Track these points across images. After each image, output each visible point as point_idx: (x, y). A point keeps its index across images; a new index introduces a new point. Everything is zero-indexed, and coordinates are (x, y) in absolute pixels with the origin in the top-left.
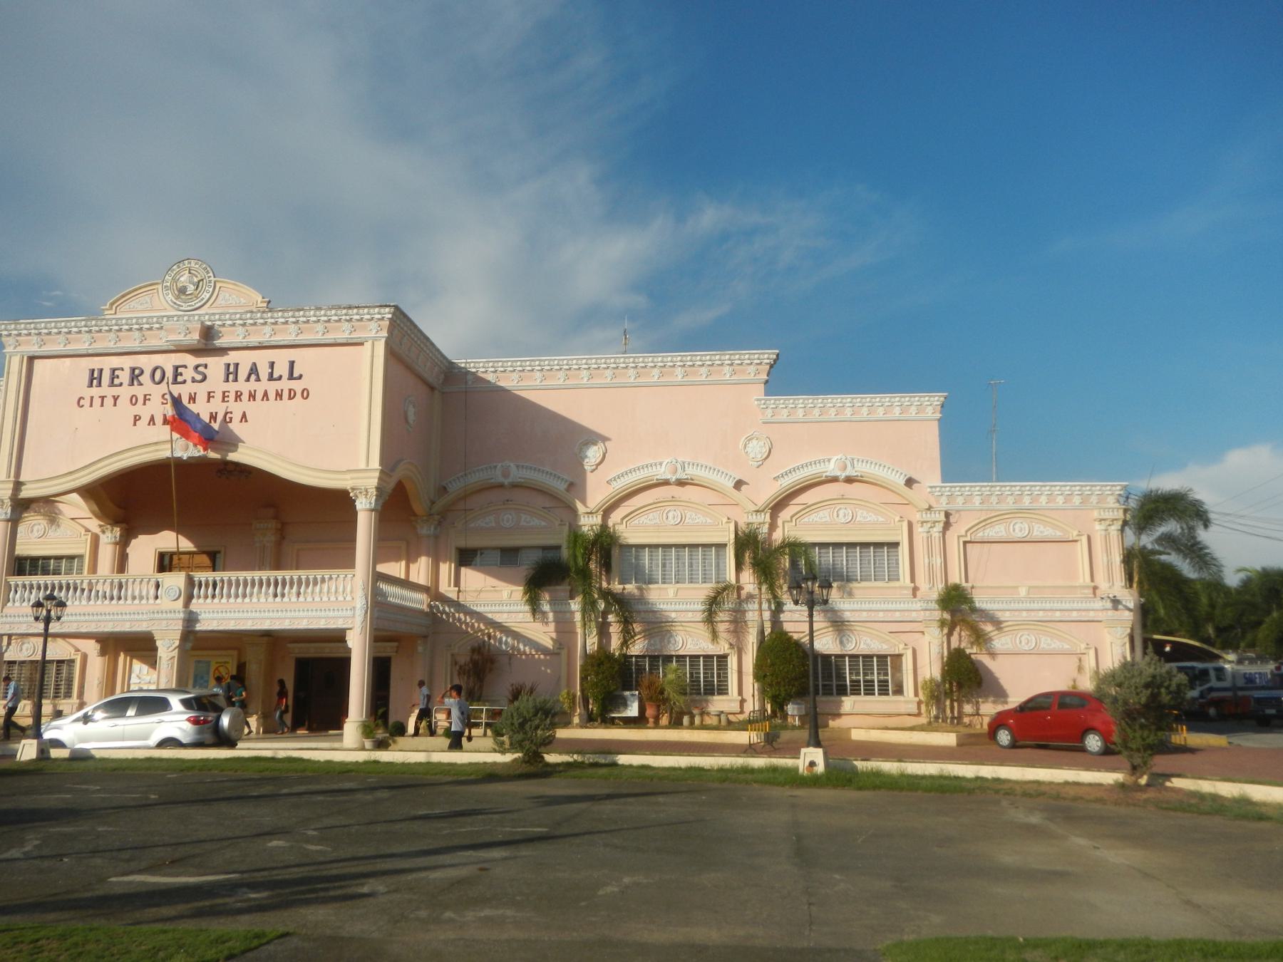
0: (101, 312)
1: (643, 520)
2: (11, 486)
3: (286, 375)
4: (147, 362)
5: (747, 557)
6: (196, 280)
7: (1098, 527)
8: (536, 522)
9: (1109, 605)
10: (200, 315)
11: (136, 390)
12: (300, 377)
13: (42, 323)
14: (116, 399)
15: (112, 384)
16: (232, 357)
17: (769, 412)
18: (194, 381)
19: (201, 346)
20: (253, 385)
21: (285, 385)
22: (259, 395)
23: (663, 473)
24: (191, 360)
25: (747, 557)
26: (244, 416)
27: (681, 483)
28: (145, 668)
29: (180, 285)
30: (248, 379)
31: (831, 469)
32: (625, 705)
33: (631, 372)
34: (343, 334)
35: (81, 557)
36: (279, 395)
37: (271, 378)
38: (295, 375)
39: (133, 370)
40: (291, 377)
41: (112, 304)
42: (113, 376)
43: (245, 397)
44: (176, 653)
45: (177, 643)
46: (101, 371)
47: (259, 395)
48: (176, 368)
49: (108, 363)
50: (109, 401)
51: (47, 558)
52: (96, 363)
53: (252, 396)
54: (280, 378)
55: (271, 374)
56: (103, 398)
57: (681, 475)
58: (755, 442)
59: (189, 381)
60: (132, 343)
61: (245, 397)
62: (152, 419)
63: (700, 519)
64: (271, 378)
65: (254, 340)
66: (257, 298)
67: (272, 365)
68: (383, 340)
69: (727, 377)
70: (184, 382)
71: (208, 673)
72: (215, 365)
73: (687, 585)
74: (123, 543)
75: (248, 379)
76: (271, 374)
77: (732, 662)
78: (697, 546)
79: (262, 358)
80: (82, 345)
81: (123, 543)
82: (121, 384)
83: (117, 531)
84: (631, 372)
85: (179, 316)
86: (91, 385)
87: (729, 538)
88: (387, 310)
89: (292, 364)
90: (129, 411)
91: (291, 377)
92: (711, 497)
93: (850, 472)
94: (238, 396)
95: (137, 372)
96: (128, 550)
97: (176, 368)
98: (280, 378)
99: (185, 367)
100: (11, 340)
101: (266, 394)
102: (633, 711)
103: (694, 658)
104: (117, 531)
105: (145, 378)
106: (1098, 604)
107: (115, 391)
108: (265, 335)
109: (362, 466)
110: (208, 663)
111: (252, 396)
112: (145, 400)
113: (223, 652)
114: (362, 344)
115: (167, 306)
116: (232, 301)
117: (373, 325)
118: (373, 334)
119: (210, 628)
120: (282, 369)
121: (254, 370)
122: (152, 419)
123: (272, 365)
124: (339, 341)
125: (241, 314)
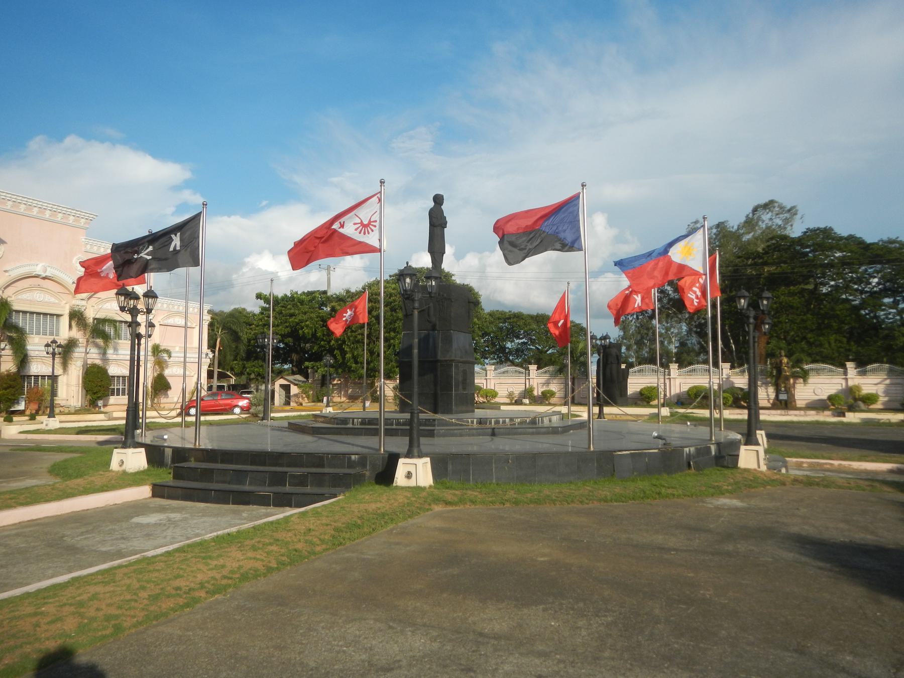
1: (26, 296)
5: (74, 324)
17: (88, 247)
23: (38, 270)
25: (74, 324)
27: (44, 278)
32: (18, 403)
33: (22, 206)
57: (48, 274)
63: (53, 300)
73: (41, 336)
77: (62, 381)
78: (45, 314)
84: (22, 206)
92: (58, 288)
102: (21, 406)
103: (43, 377)
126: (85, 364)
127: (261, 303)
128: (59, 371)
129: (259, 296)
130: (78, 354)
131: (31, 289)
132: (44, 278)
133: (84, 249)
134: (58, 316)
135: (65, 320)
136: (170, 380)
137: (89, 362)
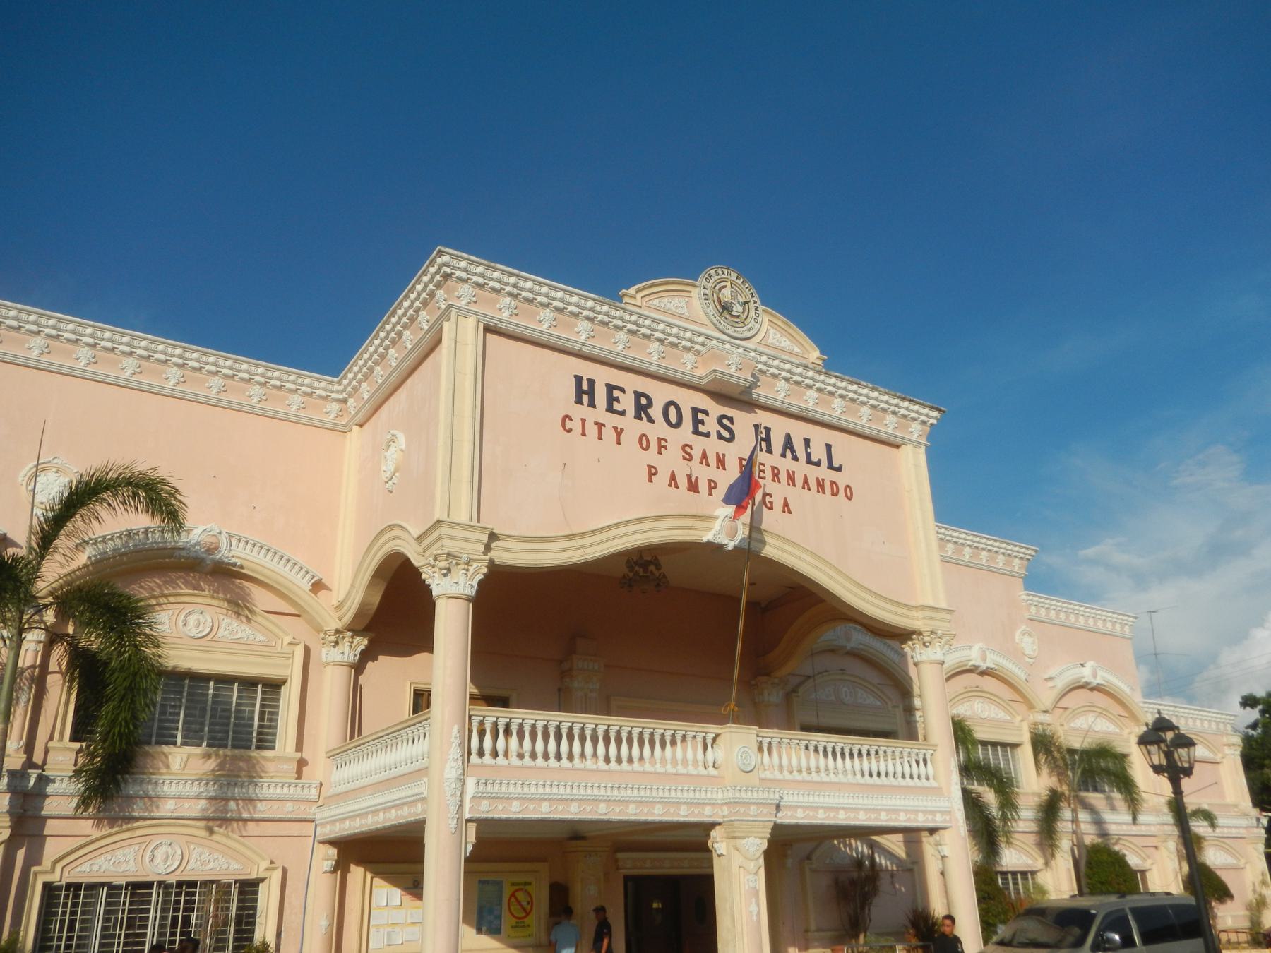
0: (620, 299)
2: (485, 538)
4: (660, 394)
6: (742, 300)
7: (1227, 751)
8: (871, 700)
9: (1255, 822)
10: (746, 349)
11: (643, 426)
12: (839, 469)
13: (530, 283)
14: (619, 432)
15: (610, 409)
16: (764, 418)
17: (1033, 610)
18: (720, 437)
19: (735, 394)
20: (786, 464)
21: (823, 472)
24: (716, 409)
25: (1042, 758)
26: (786, 504)
28: (397, 893)
29: (724, 300)
30: (783, 455)
31: (1086, 674)
34: (889, 425)
35: (274, 686)
36: (820, 485)
37: (809, 462)
38: (836, 464)
39: (638, 395)
40: (831, 467)
41: (638, 291)
42: (611, 399)
43: (783, 476)
44: (762, 861)
45: (765, 846)
46: (592, 383)
48: (695, 411)
49: (603, 376)
50: (608, 433)
51: (205, 678)
52: (588, 370)
53: (791, 478)
54: (818, 464)
55: (808, 455)
56: (600, 425)
57: (989, 664)
58: (1026, 638)
59: (714, 435)
60: (651, 355)
61: (783, 476)
62: (673, 478)
63: (1002, 715)
64: (809, 462)
65: (795, 404)
66: (814, 355)
67: (807, 442)
68: (923, 448)
69: (1000, 565)
70: (707, 435)
71: (500, 904)
72: (744, 422)
74: (358, 668)
75: (783, 455)
76: (808, 455)
79: (799, 431)
80: (580, 334)
81: (358, 668)
82: (623, 413)
83: (362, 643)
85: (720, 341)
86: (579, 401)
87: (1026, 739)
88: (935, 414)
89: (829, 447)
90: (633, 459)
91: (831, 467)
93: (1099, 681)
94: (776, 476)
95: (644, 401)
96: (361, 679)
97: (695, 411)
98: (818, 464)
99: (706, 413)
100: (466, 289)
101: (806, 481)
104: (362, 643)
105: (656, 412)
106: (1244, 822)
108: (809, 401)
109: (931, 603)
110: (499, 884)
112: (660, 447)
113: (527, 866)
114: (898, 447)
115: (705, 321)
116: (776, 348)
117: (916, 427)
118: (915, 437)
119: (793, 821)
120: (818, 453)
121: (788, 444)
122: (673, 478)
123: (807, 442)
124: (882, 436)
125: (794, 364)
126: (1080, 844)
127: (1254, 714)
128: (1040, 863)
129: (1249, 702)
130: (1064, 824)
131: (968, 694)
132: (983, 673)
133: (1027, 615)
134: (1014, 746)
135: (1026, 753)
136: (1226, 877)
137: (1088, 840)
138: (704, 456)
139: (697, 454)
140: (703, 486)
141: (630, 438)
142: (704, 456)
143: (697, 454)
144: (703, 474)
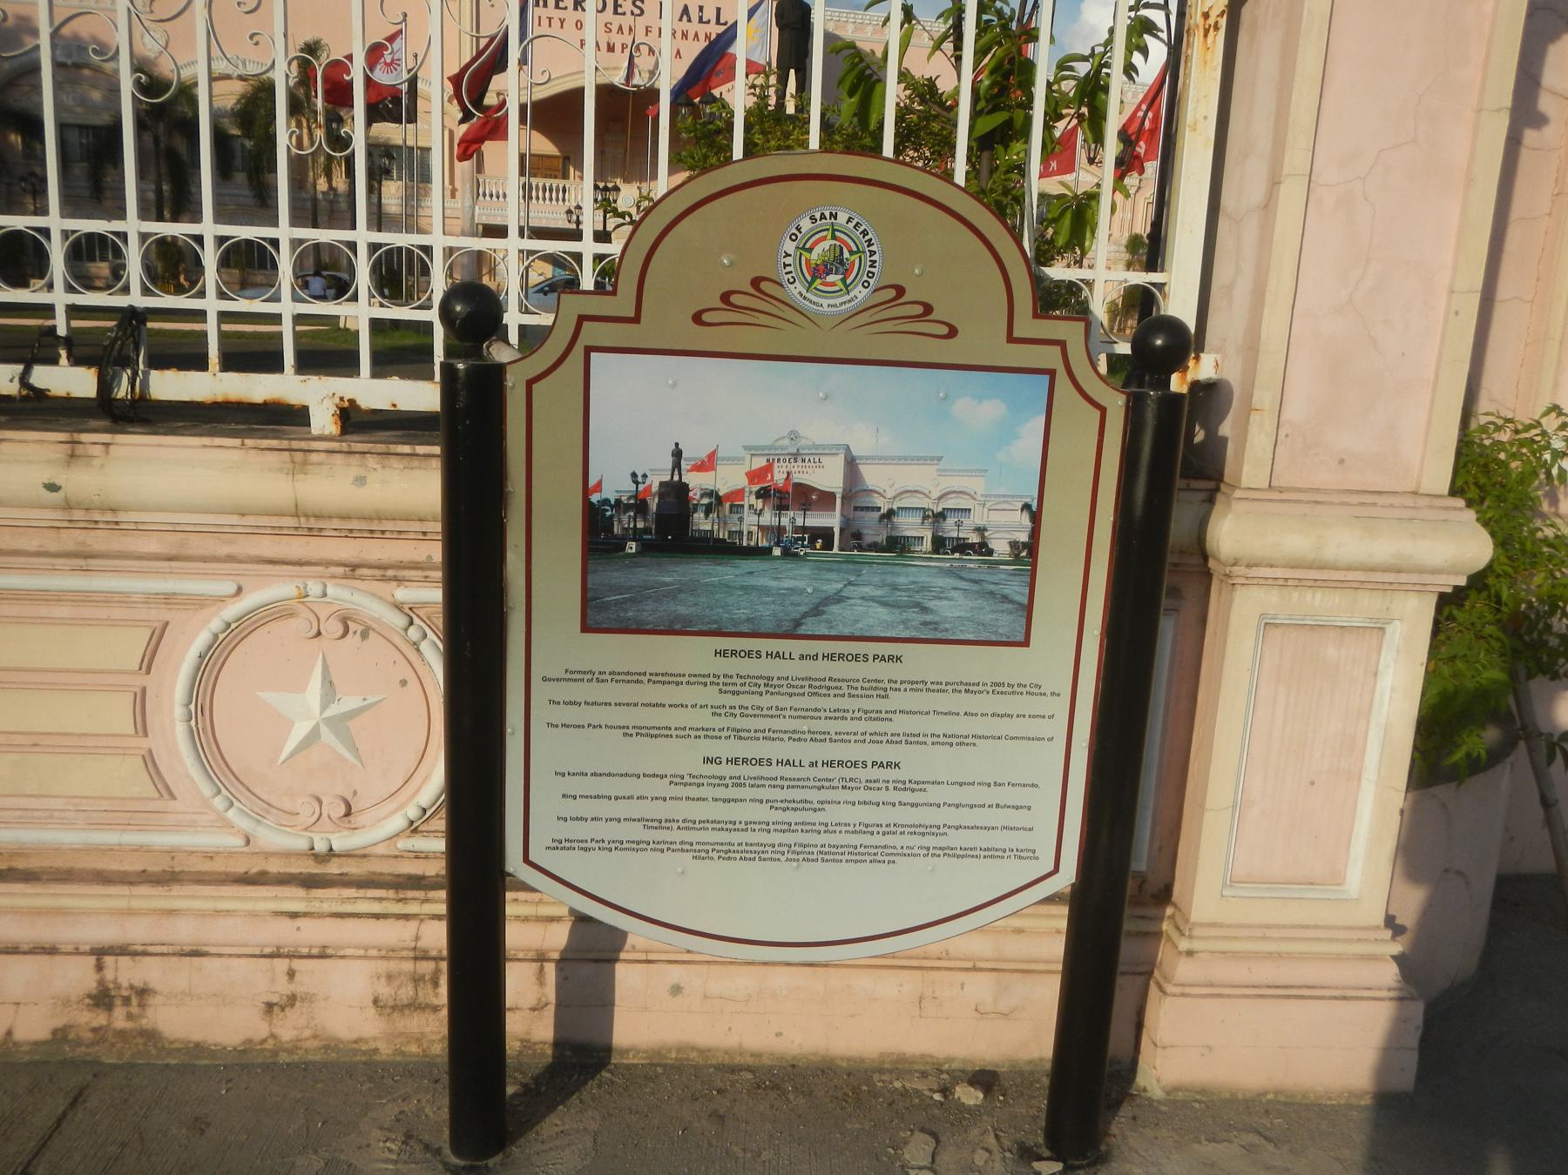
3: (714, 21)
22: (691, 36)
37: (701, 20)
47: (691, 36)
50: (556, 23)
53: (685, 35)
55: (701, 18)
67: (701, 9)
76: (701, 18)
89: (718, 10)
101: (696, 35)
107: (561, 14)
111: (685, 35)
123: (701, 9)
138: (620, 28)
139: (615, 28)
140: (618, 48)
141: (570, 24)
142: (620, 28)
143: (615, 28)
144: (618, 40)
